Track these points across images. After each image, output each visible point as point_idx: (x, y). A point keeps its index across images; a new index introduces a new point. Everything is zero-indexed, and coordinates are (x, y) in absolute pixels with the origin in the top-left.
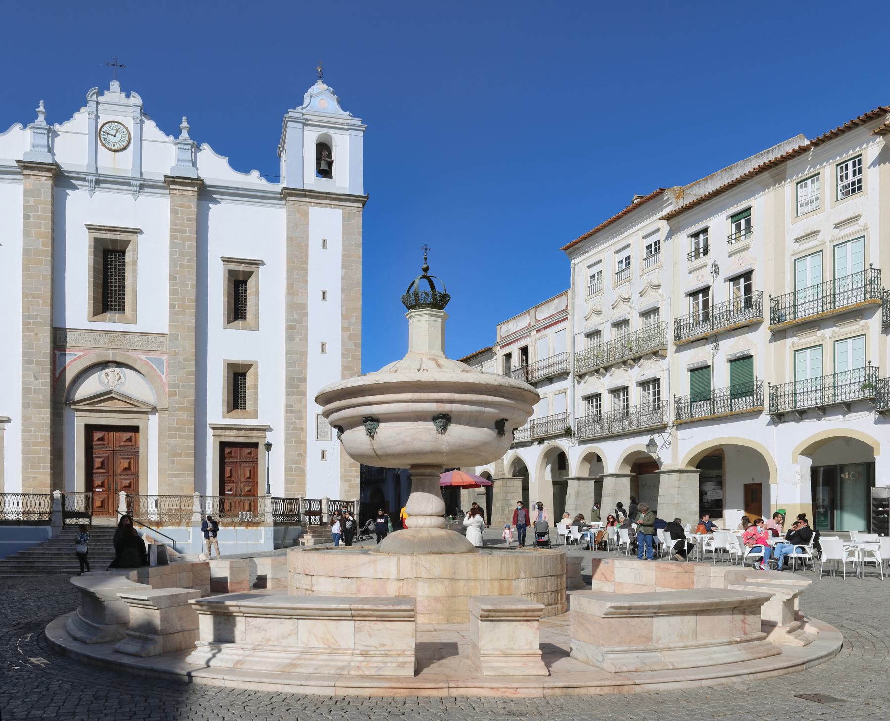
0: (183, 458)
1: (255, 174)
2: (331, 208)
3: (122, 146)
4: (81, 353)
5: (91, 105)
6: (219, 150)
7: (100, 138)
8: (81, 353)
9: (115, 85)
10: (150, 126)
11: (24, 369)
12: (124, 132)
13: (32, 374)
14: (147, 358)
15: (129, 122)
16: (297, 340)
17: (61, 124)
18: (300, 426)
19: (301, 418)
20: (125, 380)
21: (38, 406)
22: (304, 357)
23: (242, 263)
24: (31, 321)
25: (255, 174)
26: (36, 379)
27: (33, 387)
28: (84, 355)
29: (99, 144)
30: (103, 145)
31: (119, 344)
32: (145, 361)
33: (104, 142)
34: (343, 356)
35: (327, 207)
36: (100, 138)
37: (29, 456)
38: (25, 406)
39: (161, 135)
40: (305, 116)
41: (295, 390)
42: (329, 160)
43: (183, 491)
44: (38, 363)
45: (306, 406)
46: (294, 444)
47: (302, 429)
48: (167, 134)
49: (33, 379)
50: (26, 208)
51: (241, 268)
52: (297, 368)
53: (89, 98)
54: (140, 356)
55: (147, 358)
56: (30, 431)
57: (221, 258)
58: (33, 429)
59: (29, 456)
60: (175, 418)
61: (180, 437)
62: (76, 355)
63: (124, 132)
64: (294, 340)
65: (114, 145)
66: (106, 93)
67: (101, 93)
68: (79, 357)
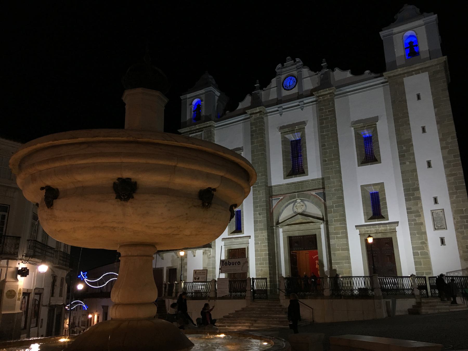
0: (340, 252)
4: (282, 197)
8: (282, 197)
10: (306, 71)
11: (254, 211)
12: (294, 79)
13: (258, 212)
14: (316, 193)
15: (295, 73)
16: (408, 163)
17: (266, 87)
18: (420, 222)
19: (420, 216)
20: (306, 208)
21: (261, 229)
22: (415, 174)
24: (256, 186)
26: (260, 215)
27: (259, 220)
28: (283, 198)
30: (285, 89)
31: (300, 188)
32: (315, 195)
33: (285, 88)
34: (446, 167)
37: (259, 257)
38: (256, 230)
41: (412, 197)
44: (260, 206)
45: (422, 207)
46: (417, 235)
47: (422, 224)
49: (258, 216)
50: (251, 132)
52: (410, 182)
54: (312, 193)
55: (316, 193)
56: (258, 243)
58: (259, 242)
59: (259, 257)
60: (333, 227)
61: (337, 238)
62: (279, 199)
63: (294, 79)
64: (406, 164)
68: (282, 199)
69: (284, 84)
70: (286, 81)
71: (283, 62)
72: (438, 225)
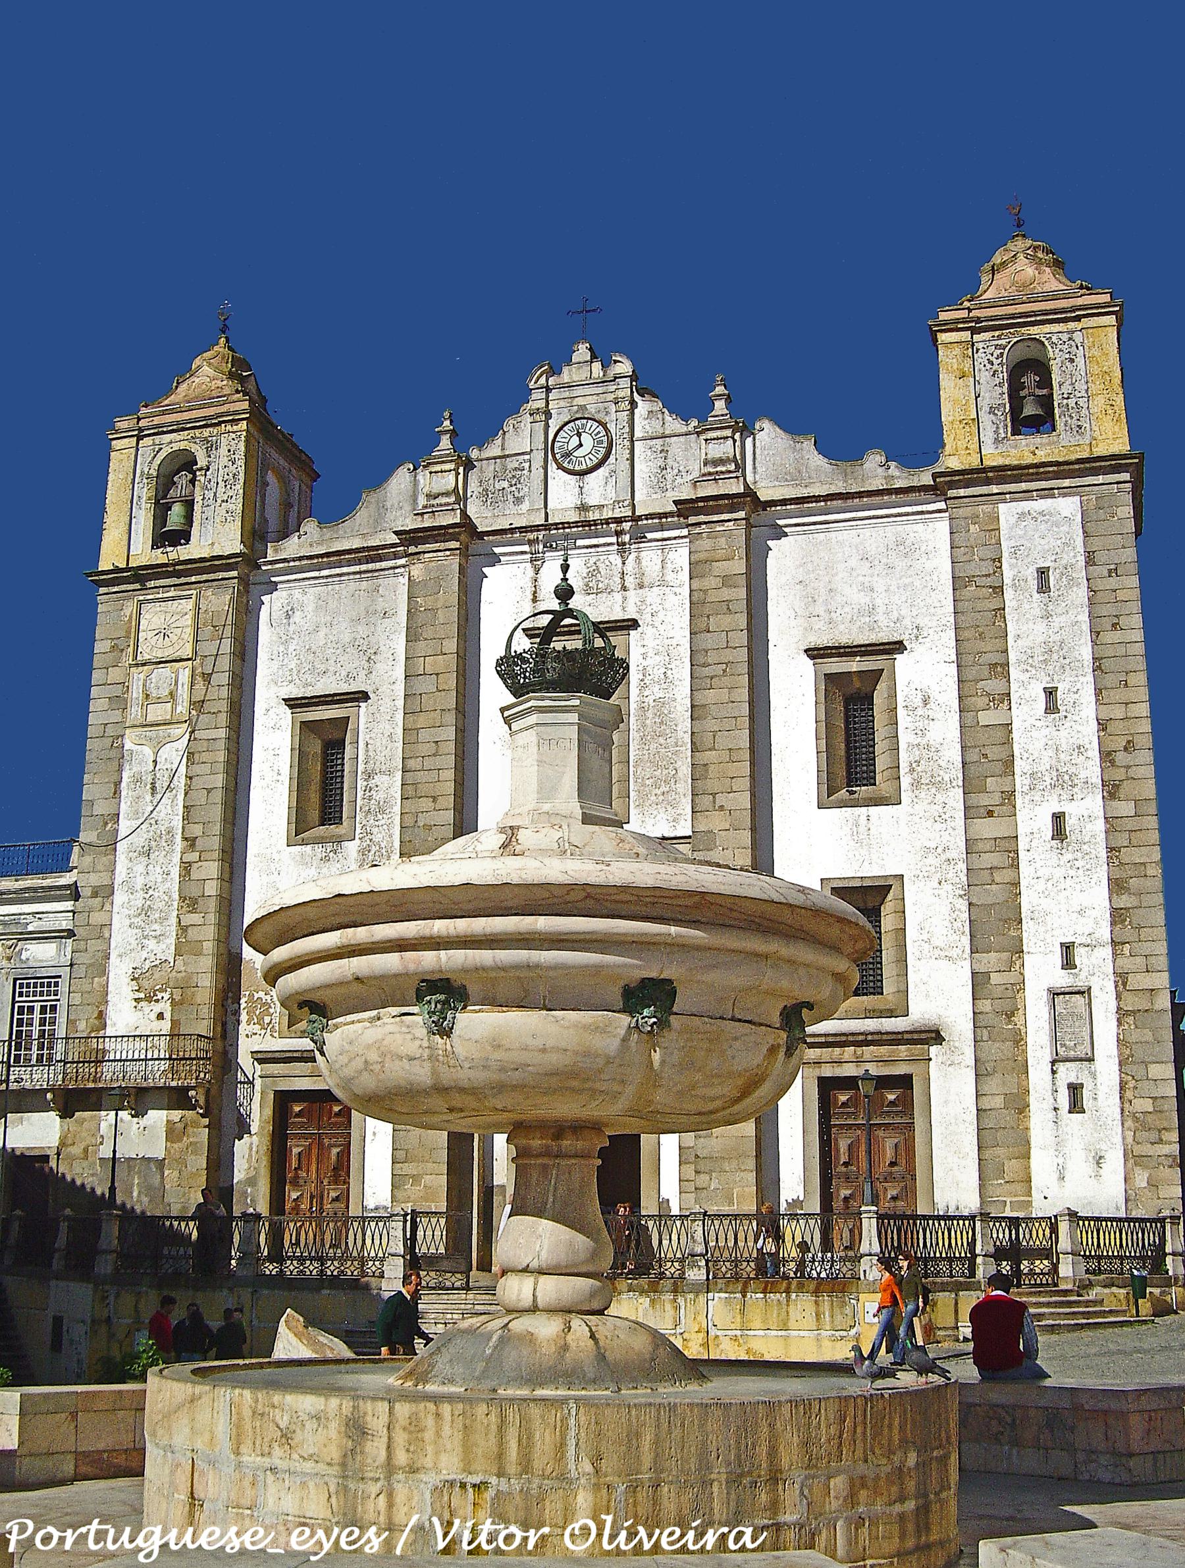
1: (873, 459)
2: (1053, 496)
3: (596, 461)
5: (537, 401)
6: (792, 427)
7: (554, 455)
9: (582, 352)
12: (599, 433)
17: (480, 447)
23: (854, 654)
25: (873, 459)
29: (552, 467)
35: (1042, 497)
36: (554, 455)
39: (674, 424)
40: (973, 314)
42: (1044, 392)
43: (731, 1203)
48: (686, 420)
51: (854, 665)
53: (532, 385)
57: (806, 651)
63: (599, 433)
65: (580, 463)
66: (565, 370)
67: (554, 371)
69: (557, 445)
70: (566, 435)
71: (558, 362)
72: (1068, 1043)
